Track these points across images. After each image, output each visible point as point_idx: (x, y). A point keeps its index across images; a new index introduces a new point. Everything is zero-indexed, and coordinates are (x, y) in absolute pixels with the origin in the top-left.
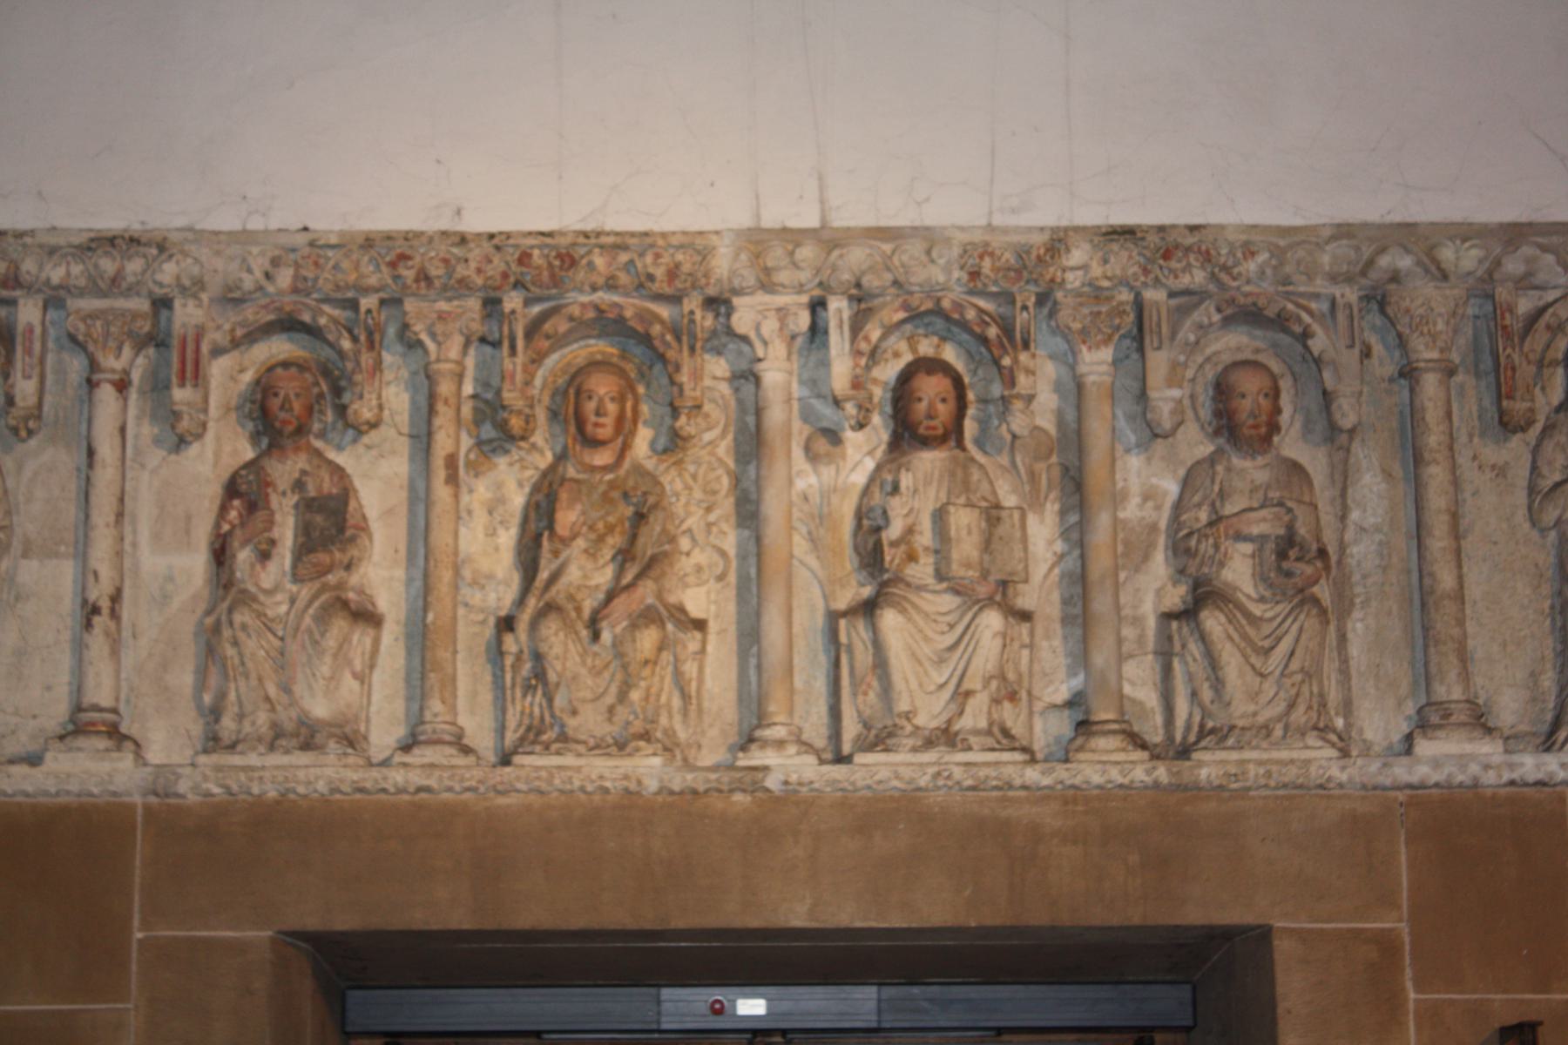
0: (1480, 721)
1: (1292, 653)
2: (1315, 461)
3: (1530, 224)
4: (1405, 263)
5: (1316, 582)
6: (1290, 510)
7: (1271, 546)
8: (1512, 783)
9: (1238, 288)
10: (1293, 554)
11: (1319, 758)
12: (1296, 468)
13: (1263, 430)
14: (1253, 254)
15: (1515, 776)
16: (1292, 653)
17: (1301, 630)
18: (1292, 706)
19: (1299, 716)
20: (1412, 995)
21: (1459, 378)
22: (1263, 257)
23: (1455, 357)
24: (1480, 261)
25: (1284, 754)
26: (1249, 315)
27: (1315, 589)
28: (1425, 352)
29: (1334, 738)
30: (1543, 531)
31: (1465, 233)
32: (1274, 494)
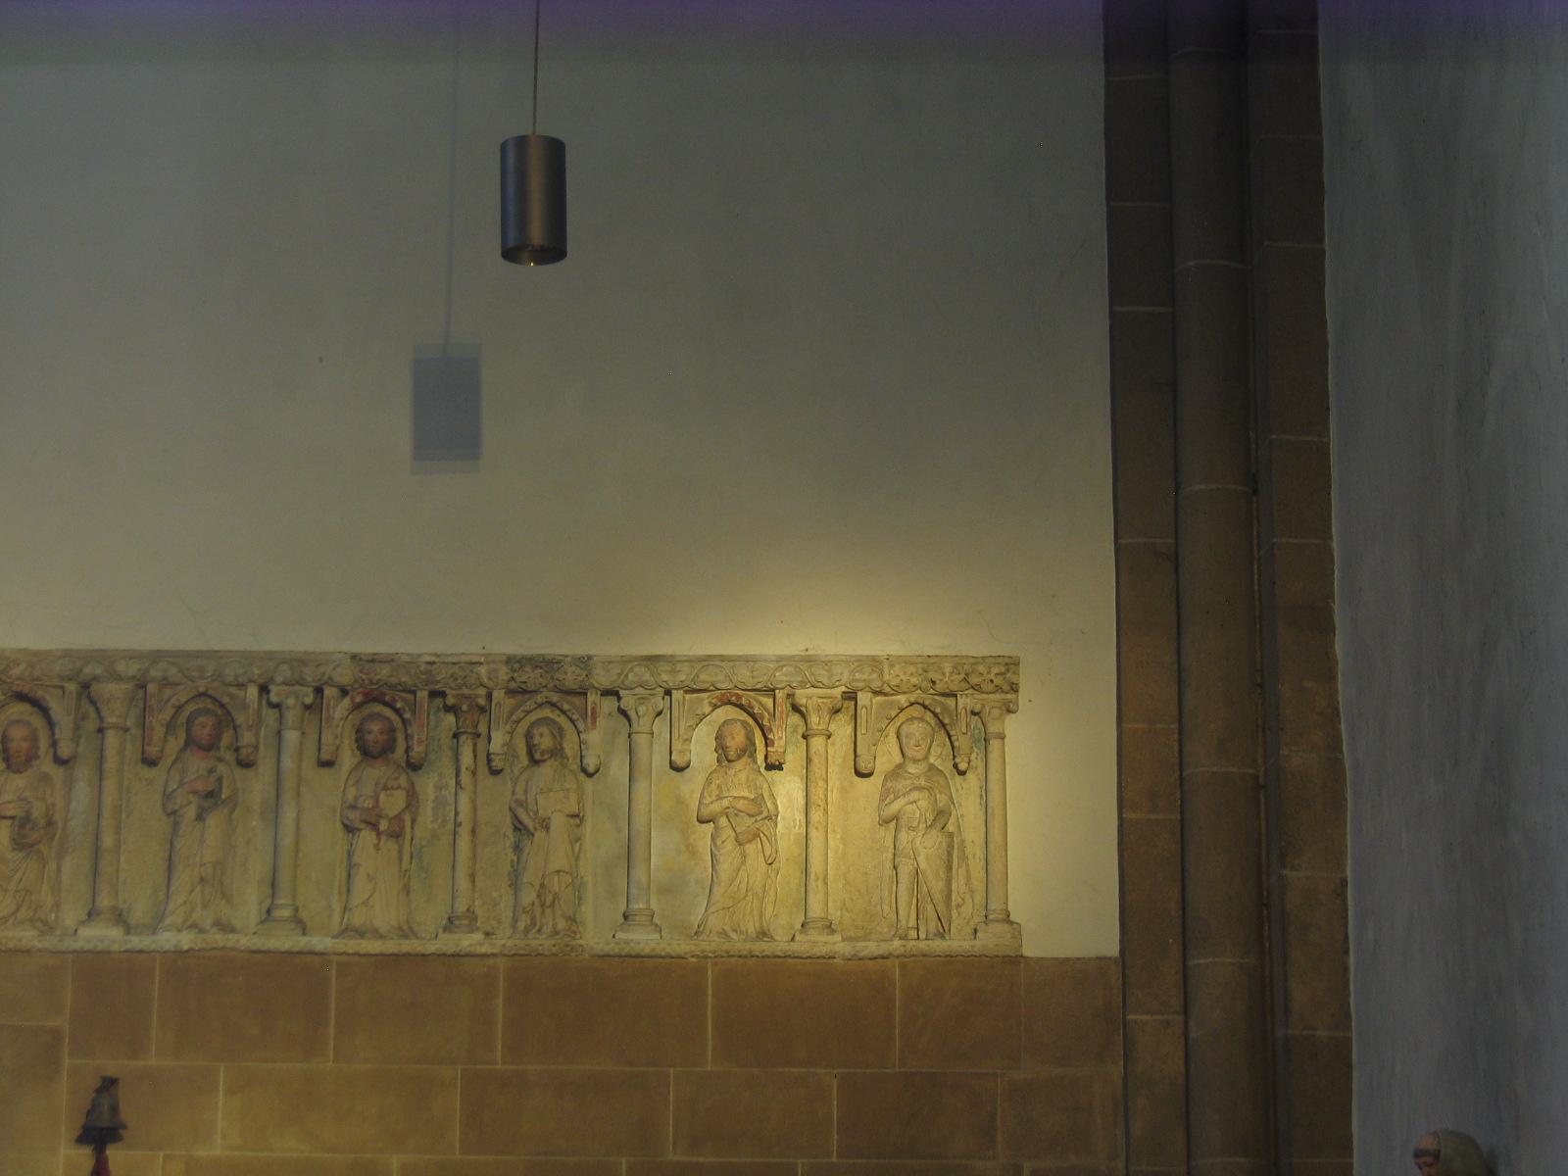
0: (119, 918)
1: (21, 879)
2: (57, 773)
3: (167, 651)
4: (98, 671)
5: (40, 842)
6: (30, 803)
7: (16, 823)
8: (126, 951)
9: (12, 683)
10: (28, 826)
11: (28, 936)
12: (46, 778)
13: (23, 759)
14: (18, 665)
15: (129, 946)
16: (21, 879)
17: (26, 868)
18: (18, 909)
19: (23, 914)
20: (67, 1061)
21: (133, 731)
22: (23, 667)
23: (129, 723)
24: (139, 670)
25: (10, 934)
26: (21, 697)
27: (42, 846)
28: (111, 720)
29: (39, 925)
30: (169, 815)
31: (133, 656)
32: (27, 794)
